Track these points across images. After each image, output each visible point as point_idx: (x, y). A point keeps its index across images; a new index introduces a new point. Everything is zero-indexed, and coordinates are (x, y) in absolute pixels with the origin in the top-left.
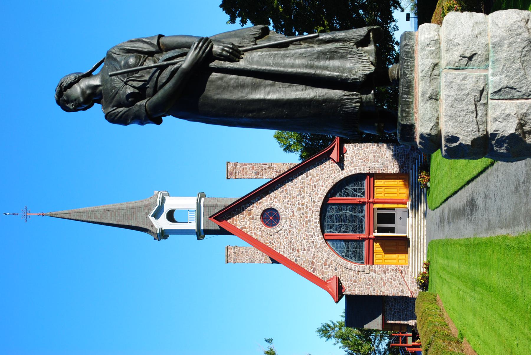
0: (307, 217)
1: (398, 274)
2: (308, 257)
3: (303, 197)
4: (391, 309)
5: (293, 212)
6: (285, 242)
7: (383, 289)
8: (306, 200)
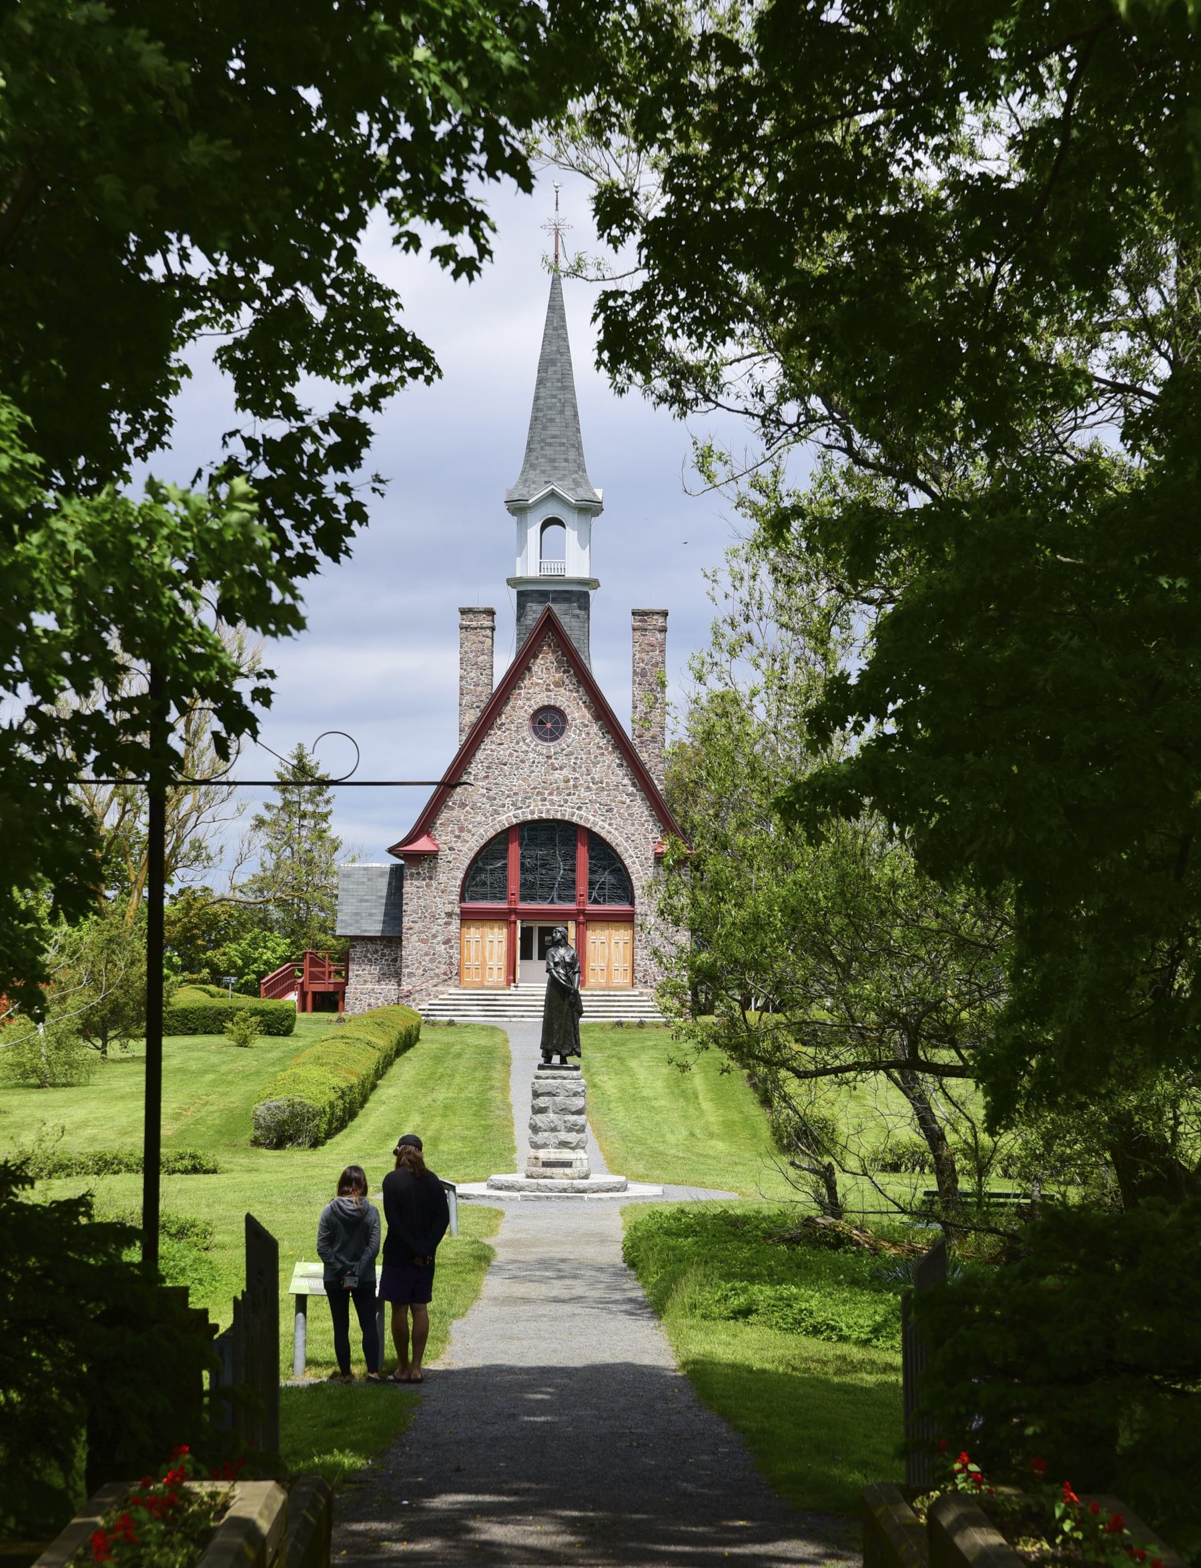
0: (551, 794)
1: (443, 967)
2: (475, 797)
3: (588, 788)
4: (376, 952)
5: (561, 768)
7: (414, 938)
8: (583, 793)
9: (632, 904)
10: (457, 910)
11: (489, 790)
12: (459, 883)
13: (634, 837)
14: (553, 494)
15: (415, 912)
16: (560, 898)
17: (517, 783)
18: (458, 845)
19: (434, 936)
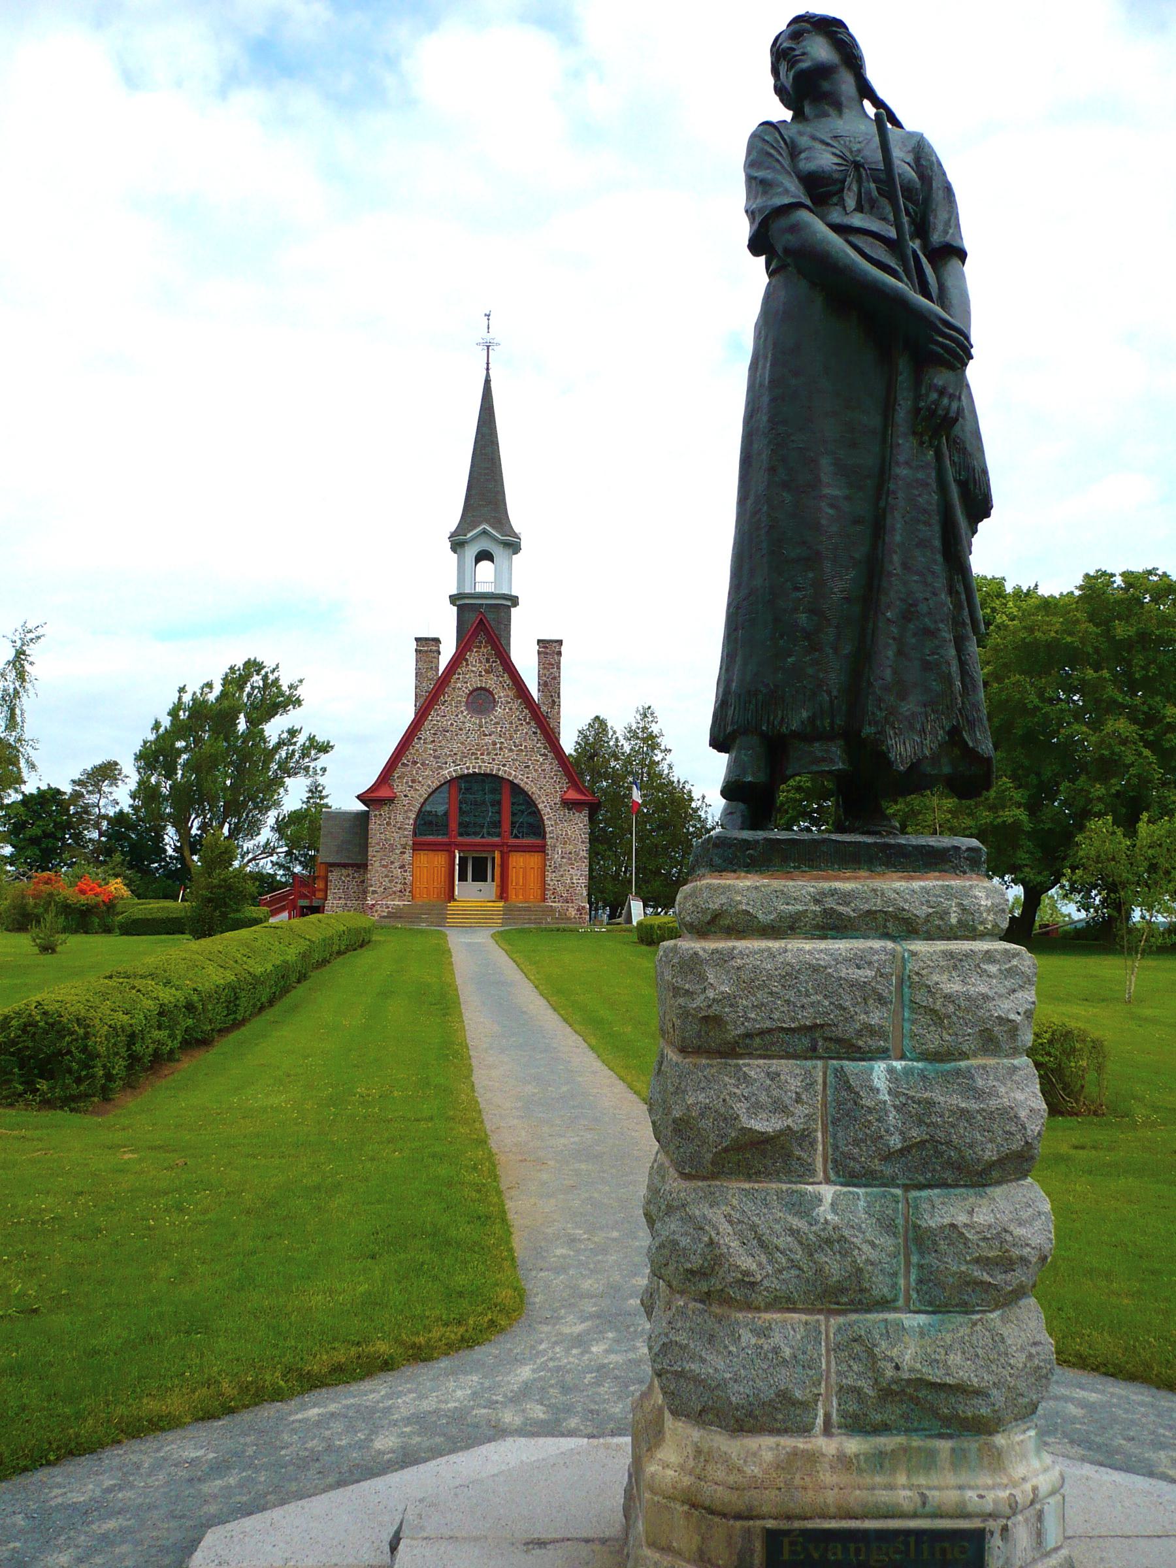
0: (482, 754)
1: (399, 887)
3: (511, 750)
4: (348, 875)
6: (445, 723)
7: (377, 864)
9: (544, 838)
10: (411, 843)
11: (435, 751)
12: (412, 821)
13: (545, 789)
14: (485, 532)
15: (378, 844)
16: (489, 834)
17: (456, 747)
18: (411, 794)
19: (392, 863)
